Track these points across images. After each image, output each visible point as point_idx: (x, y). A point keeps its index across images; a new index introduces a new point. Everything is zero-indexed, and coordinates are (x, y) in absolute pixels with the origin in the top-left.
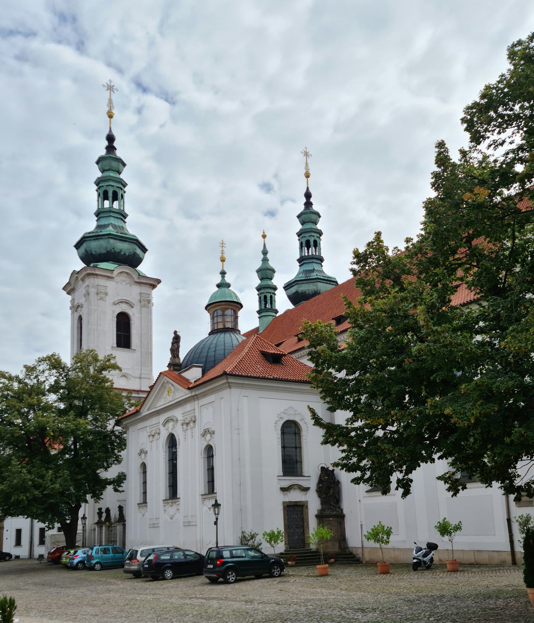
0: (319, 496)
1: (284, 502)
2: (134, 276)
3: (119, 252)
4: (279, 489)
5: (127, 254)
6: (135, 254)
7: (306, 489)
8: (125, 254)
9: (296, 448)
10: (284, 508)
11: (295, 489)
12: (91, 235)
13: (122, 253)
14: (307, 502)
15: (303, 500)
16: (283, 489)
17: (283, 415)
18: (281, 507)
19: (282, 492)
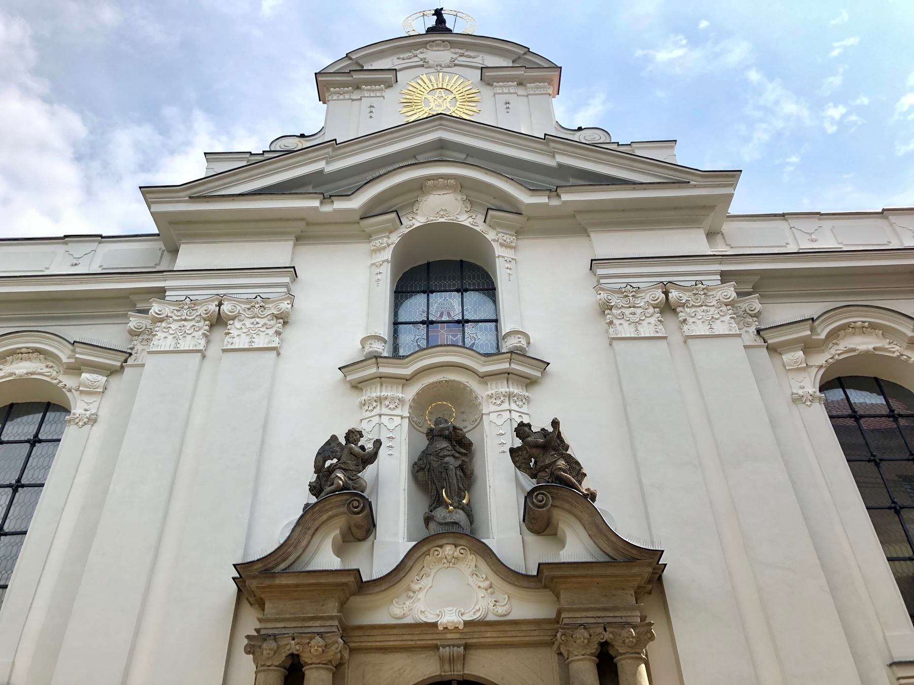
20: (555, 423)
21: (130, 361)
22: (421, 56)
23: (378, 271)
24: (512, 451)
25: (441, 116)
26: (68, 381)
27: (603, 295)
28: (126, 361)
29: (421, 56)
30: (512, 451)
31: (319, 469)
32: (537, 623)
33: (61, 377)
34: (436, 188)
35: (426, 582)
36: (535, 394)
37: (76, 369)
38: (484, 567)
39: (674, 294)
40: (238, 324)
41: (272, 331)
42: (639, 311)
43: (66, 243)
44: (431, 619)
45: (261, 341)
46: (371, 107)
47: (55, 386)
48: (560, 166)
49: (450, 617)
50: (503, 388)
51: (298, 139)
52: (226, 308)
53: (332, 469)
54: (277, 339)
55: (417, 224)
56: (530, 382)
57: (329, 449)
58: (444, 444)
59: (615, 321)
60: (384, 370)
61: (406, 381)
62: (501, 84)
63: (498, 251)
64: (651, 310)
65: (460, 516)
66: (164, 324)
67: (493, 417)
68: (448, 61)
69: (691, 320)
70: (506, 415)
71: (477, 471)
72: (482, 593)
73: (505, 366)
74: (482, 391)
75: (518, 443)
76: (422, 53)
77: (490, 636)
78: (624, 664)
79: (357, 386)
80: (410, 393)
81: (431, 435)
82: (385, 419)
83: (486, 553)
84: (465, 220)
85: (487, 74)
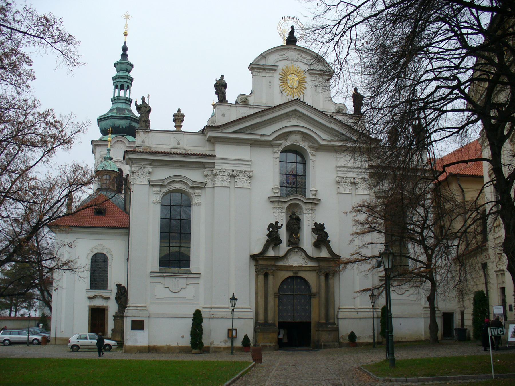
0: (117, 302)
1: (89, 306)
2: (126, 142)
3: (119, 127)
4: (87, 298)
5: (124, 127)
6: (130, 126)
7: (107, 298)
8: (123, 127)
9: (104, 271)
10: (89, 309)
11: (98, 298)
12: (103, 117)
13: (121, 127)
14: (107, 306)
15: (105, 305)
16: (90, 298)
17: (94, 250)
18: (87, 309)
19: (88, 300)
20: (324, 224)
21: (207, 186)
23: (276, 161)
24: (312, 229)
26: (191, 191)
27: (338, 179)
28: (205, 186)
30: (312, 229)
31: (268, 230)
33: (189, 190)
34: (295, 133)
36: (317, 207)
37: (193, 188)
39: (356, 180)
41: (248, 182)
42: (347, 184)
43: (173, 133)
44: (291, 265)
45: (246, 185)
46: (270, 82)
47: (188, 192)
48: (332, 128)
49: (295, 264)
50: (310, 207)
54: (249, 184)
55: (288, 144)
56: (316, 204)
57: (271, 226)
59: (340, 187)
60: (280, 200)
61: (285, 202)
63: (311, 157)
64: (349, 184)
66: (217, 177)
67: (307, 215)
69: (359, 188)
71: (302, 228)
72: (302, 260)
73: (312, 202)
74: (304, 207)
75: (314, 227)
76: (286, 53)
77: (304, 269)
78: (330, 277)
79: (271, 202)
80: (286, 206)
81: (290, 216)
82: (280, 213)
83: (304, 252)
84: (302, 144)
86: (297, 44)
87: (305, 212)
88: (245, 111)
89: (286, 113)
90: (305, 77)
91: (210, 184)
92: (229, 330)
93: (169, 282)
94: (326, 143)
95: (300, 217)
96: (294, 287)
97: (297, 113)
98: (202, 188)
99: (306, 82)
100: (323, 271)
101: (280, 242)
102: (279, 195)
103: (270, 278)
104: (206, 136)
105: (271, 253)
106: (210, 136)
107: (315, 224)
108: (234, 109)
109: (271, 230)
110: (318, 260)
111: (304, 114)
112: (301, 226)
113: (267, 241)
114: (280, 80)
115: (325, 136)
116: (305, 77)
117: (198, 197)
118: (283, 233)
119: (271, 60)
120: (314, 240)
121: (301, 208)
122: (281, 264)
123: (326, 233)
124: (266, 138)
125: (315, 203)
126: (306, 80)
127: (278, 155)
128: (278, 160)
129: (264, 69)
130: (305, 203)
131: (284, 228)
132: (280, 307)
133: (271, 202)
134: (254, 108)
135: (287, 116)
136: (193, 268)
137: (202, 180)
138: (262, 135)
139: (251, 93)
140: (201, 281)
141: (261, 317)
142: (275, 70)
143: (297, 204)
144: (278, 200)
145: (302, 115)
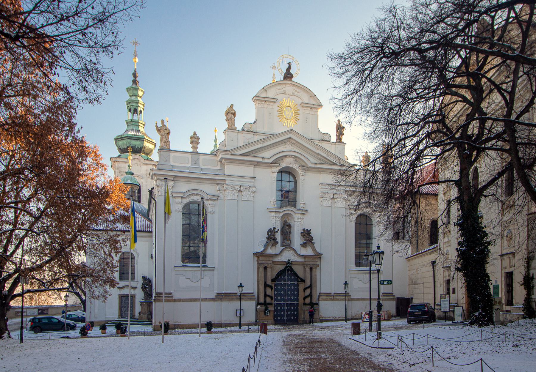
20: (310, 230)
22: (284, 89)
24: (301, 233)
25: (292, 130)
29: (284, 89)
30: (301, 233)
31: (268, 234)
32: (301, 262)
35: (284, 254)
36: (305, 217)
38: (293, 252)
40: (244, 193)
41: (252, 196)
50: (299, 216)
51: (250, 125)
52: (242, 188)
53: (270, 235)
56: (304, 214)
57: (270, 231)
58: (287, 227)
60: (277, 210)
62: (306, 109)
63: (301, 177)
65: (289, 242)
67: (297, 222)
68: (291, 93)
70: (299, 223)
75: (303, 232)
78: (314, 270)
80: (281, 214)
81: (284, 224)
83: (294, 250)
85: (303, 105)
86: (293, 79)
87: (296, 220)
88: (250, 137)
89: (283, 140)
90: (299, 110)
91: (222, 197)
92: (237, 310)
93: (190, 273)
94: (313, 166)
95: (292, 224)
96: (286, 277)
97: (291, 140)
98: (215, 200)
99: (299, 114)
100: (309, 266)
101: (277, 243)
102: (276, 206)
103: (269, 270)
104: (218, 157)
105: (270, 251)
106: (222, 158)
107: (304, 230)
108: (240, 135)
109: (270, 233)
110: (305, 256)
111: (297, 142)
112: (291, 231)
113: (267, 243)
114: (278, 111)
115: (313, 160)
116: (299, 110)
117: (212, 207)
118: (278, 236)
119: (271, 94)
120: (301, 243)
121: (292, 217)
122: (277, 259)
123: (311, 236)
124: (266, 161)
125: (304, 212)
126: (300, 112)
127: (275, 175)
128: (276, 179)
129: (265, 101)
130: (296, 213)
131: (279, 232)
132: (276, 293)
133: (270, 212)
134: (257, 135)
135: (283, 142)
136: (209, 263)
137: (217, 193)
138: (263, 158)
139: (254, 123)
140: (215, 272)
141: (262, 300)
142: (275, 102)
143: (289, 214)
144: (275, 210)
145: (295, 142)
